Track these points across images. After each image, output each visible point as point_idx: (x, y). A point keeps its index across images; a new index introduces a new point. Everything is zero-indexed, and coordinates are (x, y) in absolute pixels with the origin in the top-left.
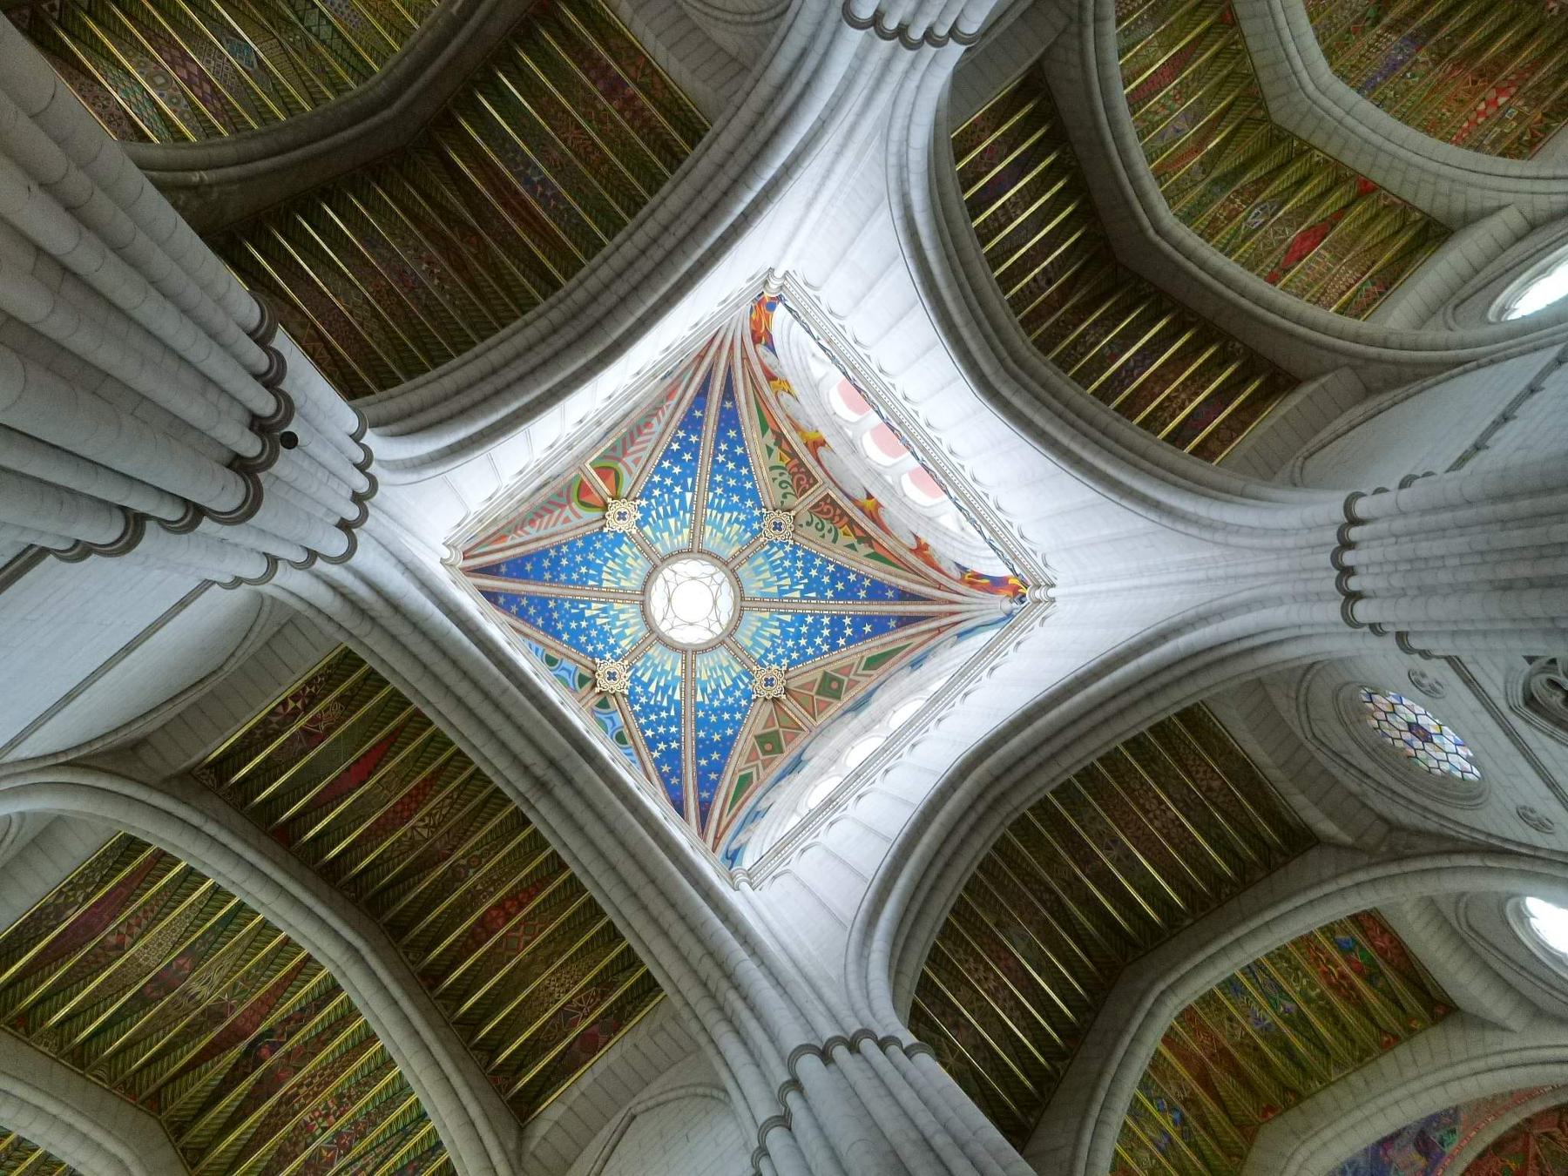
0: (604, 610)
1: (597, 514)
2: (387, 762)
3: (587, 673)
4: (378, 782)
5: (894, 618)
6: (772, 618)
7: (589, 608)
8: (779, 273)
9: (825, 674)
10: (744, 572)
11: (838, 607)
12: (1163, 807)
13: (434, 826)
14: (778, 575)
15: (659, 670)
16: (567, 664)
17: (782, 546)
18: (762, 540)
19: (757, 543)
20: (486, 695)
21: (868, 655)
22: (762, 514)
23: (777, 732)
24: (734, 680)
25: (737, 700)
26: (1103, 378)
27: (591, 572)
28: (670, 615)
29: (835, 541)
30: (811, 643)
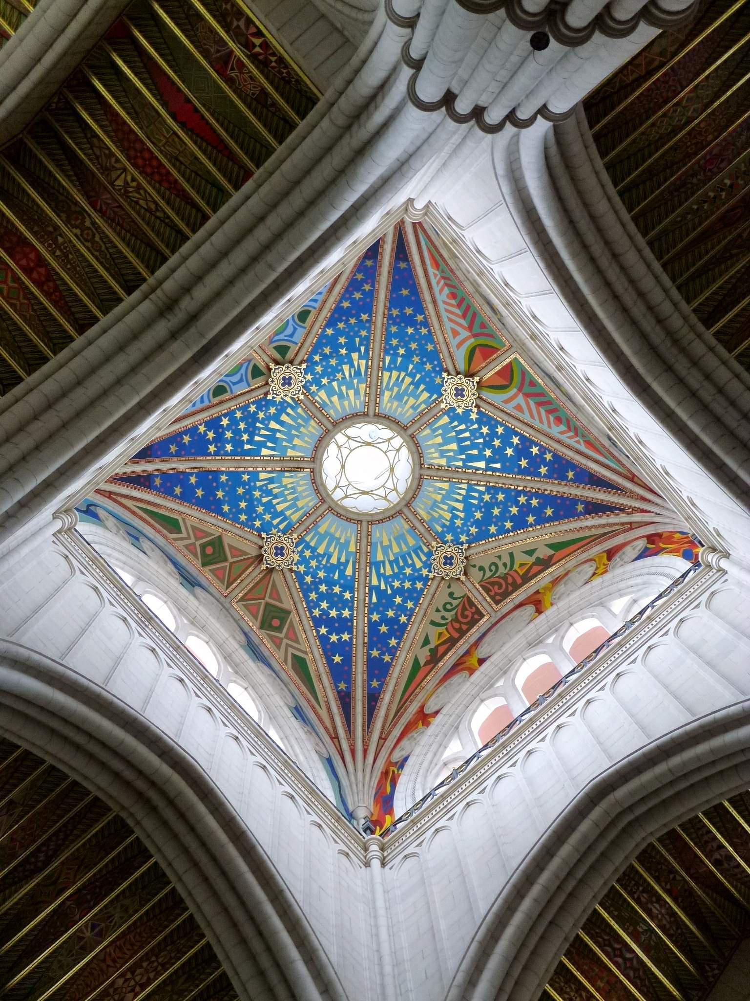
0: (358, 373)
1: (462, 366)
2: (195, 143)
3: (290, 355)
4: (175, 133)
5: (349, 688)
6: (348, 554)
7: (360, 357)
8: (724, 563)
9: (289, 612)
10: (399, 525)
11: (360, 627)
12: (138, 989)
13: (126, 192)
14: (396, 561)
15: (294, 432)
16: (300, 334)
17: (428, 565)
18: (434, 544)
19: (430, 539)
20: (267, 247)
21: (309, 659)
22: (462, 544)
23: (226, 560)
24: (282, 513)
25: (260, 517)
26: (613, 923)
27: (399, 359)
28: (353, 445)
29: (433, 623)
30: (321, 597)
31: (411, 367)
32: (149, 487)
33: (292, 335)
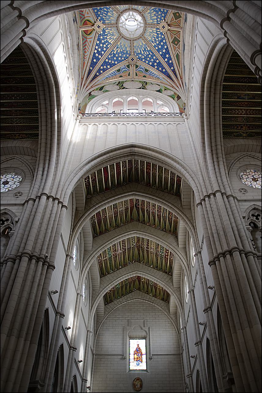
0: (117, 48)
1: (94, 32)
7: (114, 51)
9: (173, 13)
13: (125, 166)
15: (140, 47)
24: (156, 33)
25: (161, 37)
27: (106, 44)
28: (130, 32)
31: (105, 40)
32: (174, 69)
33: (124, 68)
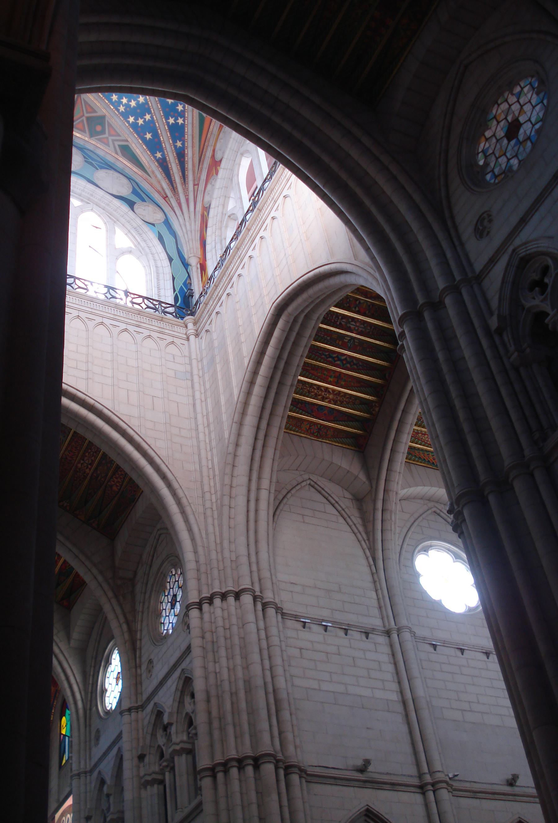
5: (163, 155)
9: (103, 117)
12: (89, 466)
